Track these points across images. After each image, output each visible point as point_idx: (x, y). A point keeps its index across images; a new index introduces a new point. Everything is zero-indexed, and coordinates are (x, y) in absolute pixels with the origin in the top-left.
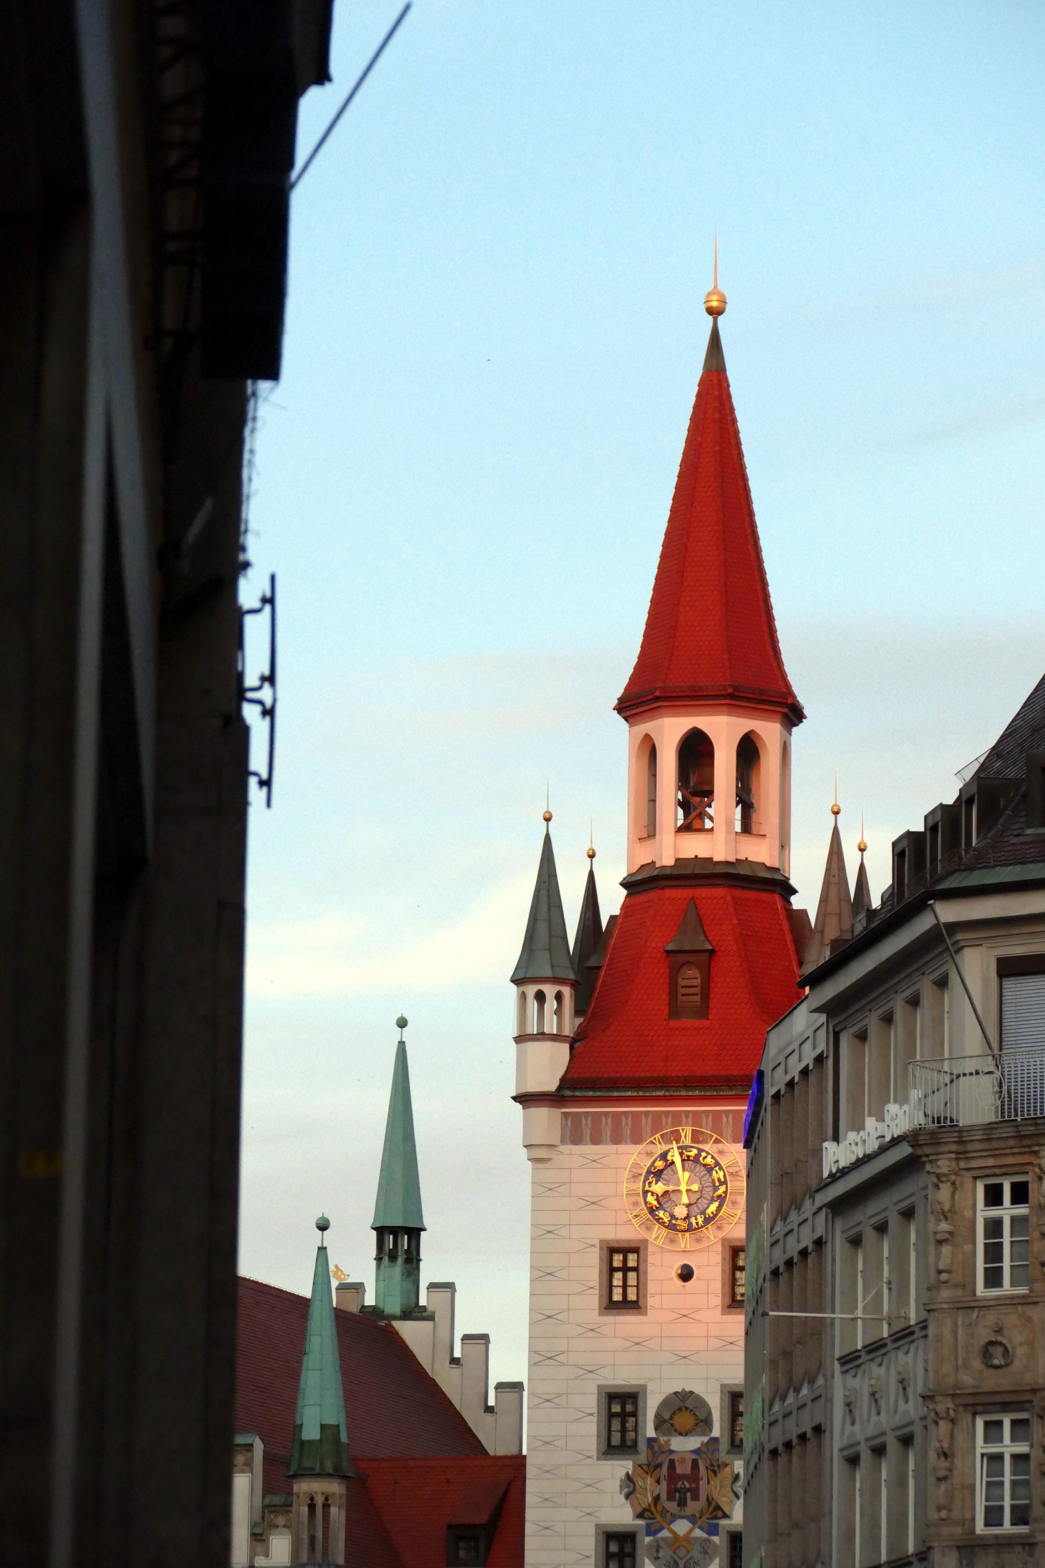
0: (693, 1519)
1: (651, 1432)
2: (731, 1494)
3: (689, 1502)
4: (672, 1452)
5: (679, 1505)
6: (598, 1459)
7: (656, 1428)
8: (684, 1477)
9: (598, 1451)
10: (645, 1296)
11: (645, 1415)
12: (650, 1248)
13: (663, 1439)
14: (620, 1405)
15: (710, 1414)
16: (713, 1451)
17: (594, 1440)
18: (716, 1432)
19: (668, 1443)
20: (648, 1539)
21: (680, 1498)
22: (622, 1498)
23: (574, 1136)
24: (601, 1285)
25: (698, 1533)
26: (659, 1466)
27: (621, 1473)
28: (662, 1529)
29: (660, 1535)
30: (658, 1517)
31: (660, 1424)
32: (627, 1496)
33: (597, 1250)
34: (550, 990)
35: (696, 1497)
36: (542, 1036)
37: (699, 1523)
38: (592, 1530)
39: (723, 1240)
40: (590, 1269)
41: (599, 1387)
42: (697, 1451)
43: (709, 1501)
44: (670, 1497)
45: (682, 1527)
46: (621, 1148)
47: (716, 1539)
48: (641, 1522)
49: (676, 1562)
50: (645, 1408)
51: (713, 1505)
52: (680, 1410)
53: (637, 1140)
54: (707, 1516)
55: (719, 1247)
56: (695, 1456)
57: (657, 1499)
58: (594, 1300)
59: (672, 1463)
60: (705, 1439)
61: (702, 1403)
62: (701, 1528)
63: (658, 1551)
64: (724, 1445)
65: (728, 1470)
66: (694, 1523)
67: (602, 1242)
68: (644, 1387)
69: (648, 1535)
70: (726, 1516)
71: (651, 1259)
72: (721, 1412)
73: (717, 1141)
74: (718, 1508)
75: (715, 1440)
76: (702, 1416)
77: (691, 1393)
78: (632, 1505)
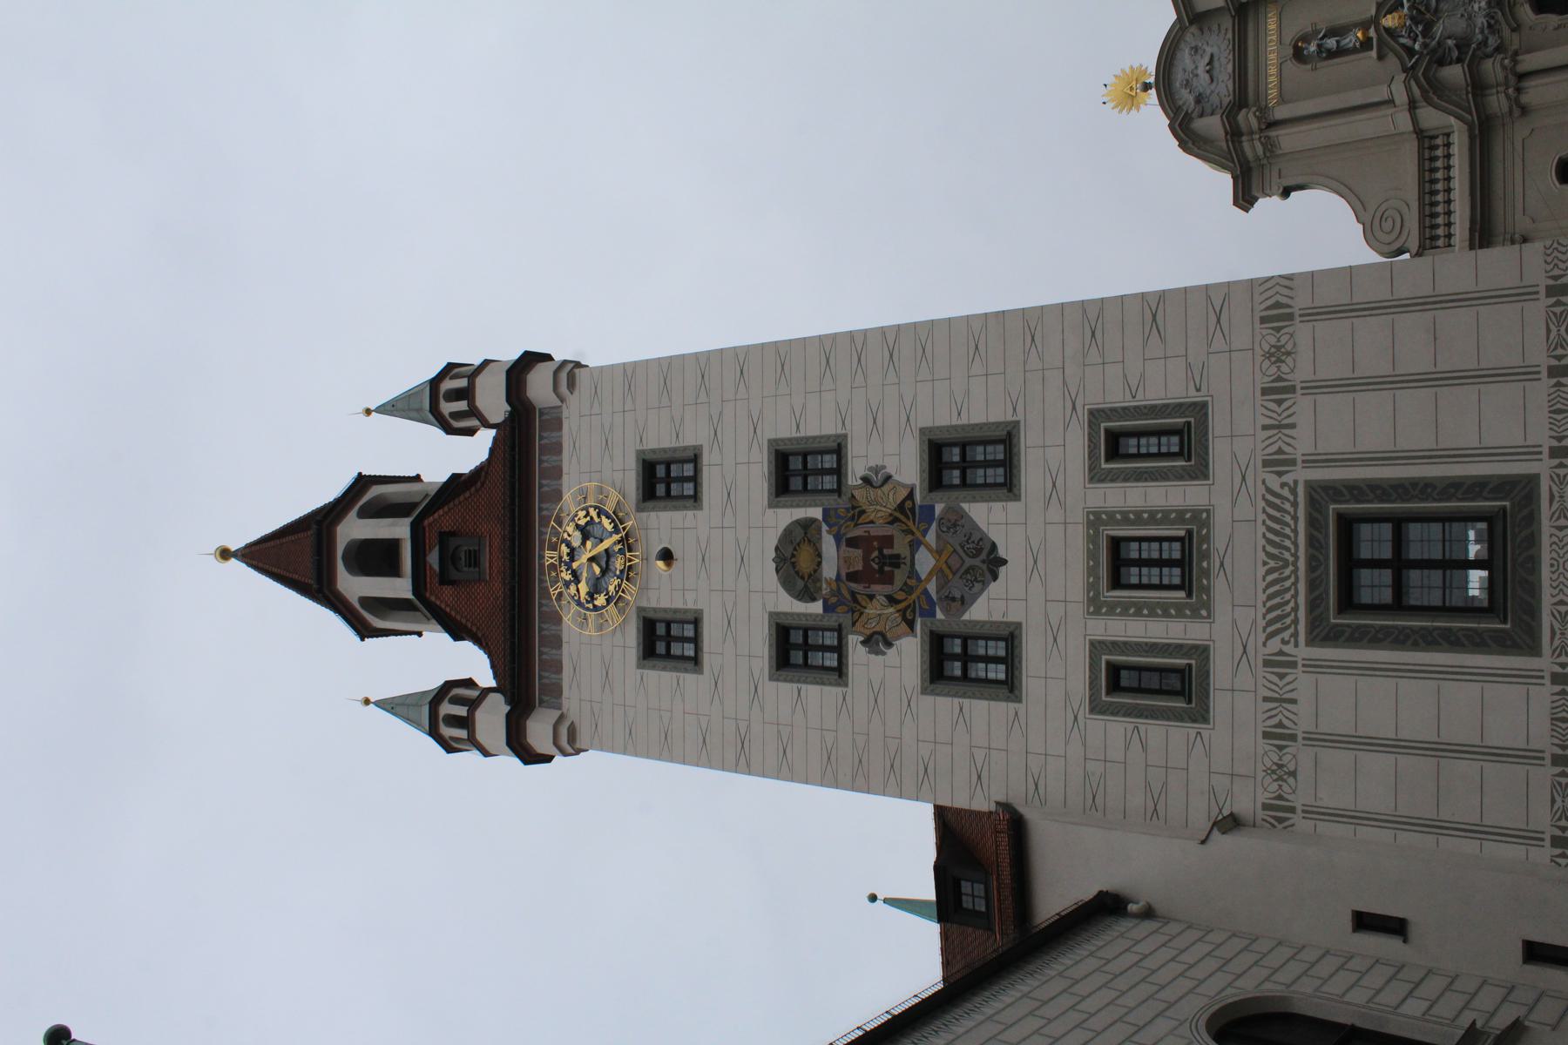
0: (915, 545)
1: (816, 608)
2: (886, 488)
3: (895, 551)
4: (838, 575)
5: (897, 566)
6: (846, 685)
7: (814, 599)
8: (866, 559)
9: (839, 685)
10: (686, 611)
11: (799, 615)
12: (644, 604)
13: (825, 590)
14: (794, 651)
15: (798, 522)
16: (839, 517)
17: (827, 689)
18: (816, 513)
19: (829, 583)
20: (940, 615)
21: (891, 565)
22: (891, 652)
23: (554, 693)
24: (676, 669)
25: (931, 537)
26: (853, 594)
27: (862, 650)
28: (926, 592)
29: (934, 597)
30: (914, 596)
31: (807, 595)
32: (889, 644)
33: (646, 671)
34: (447, 709)
35: (888, 541)
36: (466, 723)
37: (918, 534)
38: (929, 699)
39: (639, 509)
40: (661, 679)
41: (771, 679)
42: (838, 539)
43: (893, 521)
44: (889, 580)
45: (925, 562)
46: (565, 639)
47: (939, 508)
48: (919, 622)
49: (967, 572)
50: (792, 614)
51: (898, 514)
52: (793, 564)
53: (558, 620)
54: (910, 523)
55: (644, 514)
56: (843, 547)
57: (892, 600)
58: (689, 679)
59: (852, 577)
60: (825, 527)
61: (787, 535)
62: (925, 532)
63: (953, 599)
64: (831, 500)
65: (856, 493)
66: (919, 543)
67: (639, 666)
68: (771, 615)
69: (934, 615)
70: (911, 496)
71: (654, 605)
72: (798, 506)
73: (560, 524)
74: (901, 507)
75: (826, 512)
76: (799, 532)
77: (777, 549)
78: (898, 637)
